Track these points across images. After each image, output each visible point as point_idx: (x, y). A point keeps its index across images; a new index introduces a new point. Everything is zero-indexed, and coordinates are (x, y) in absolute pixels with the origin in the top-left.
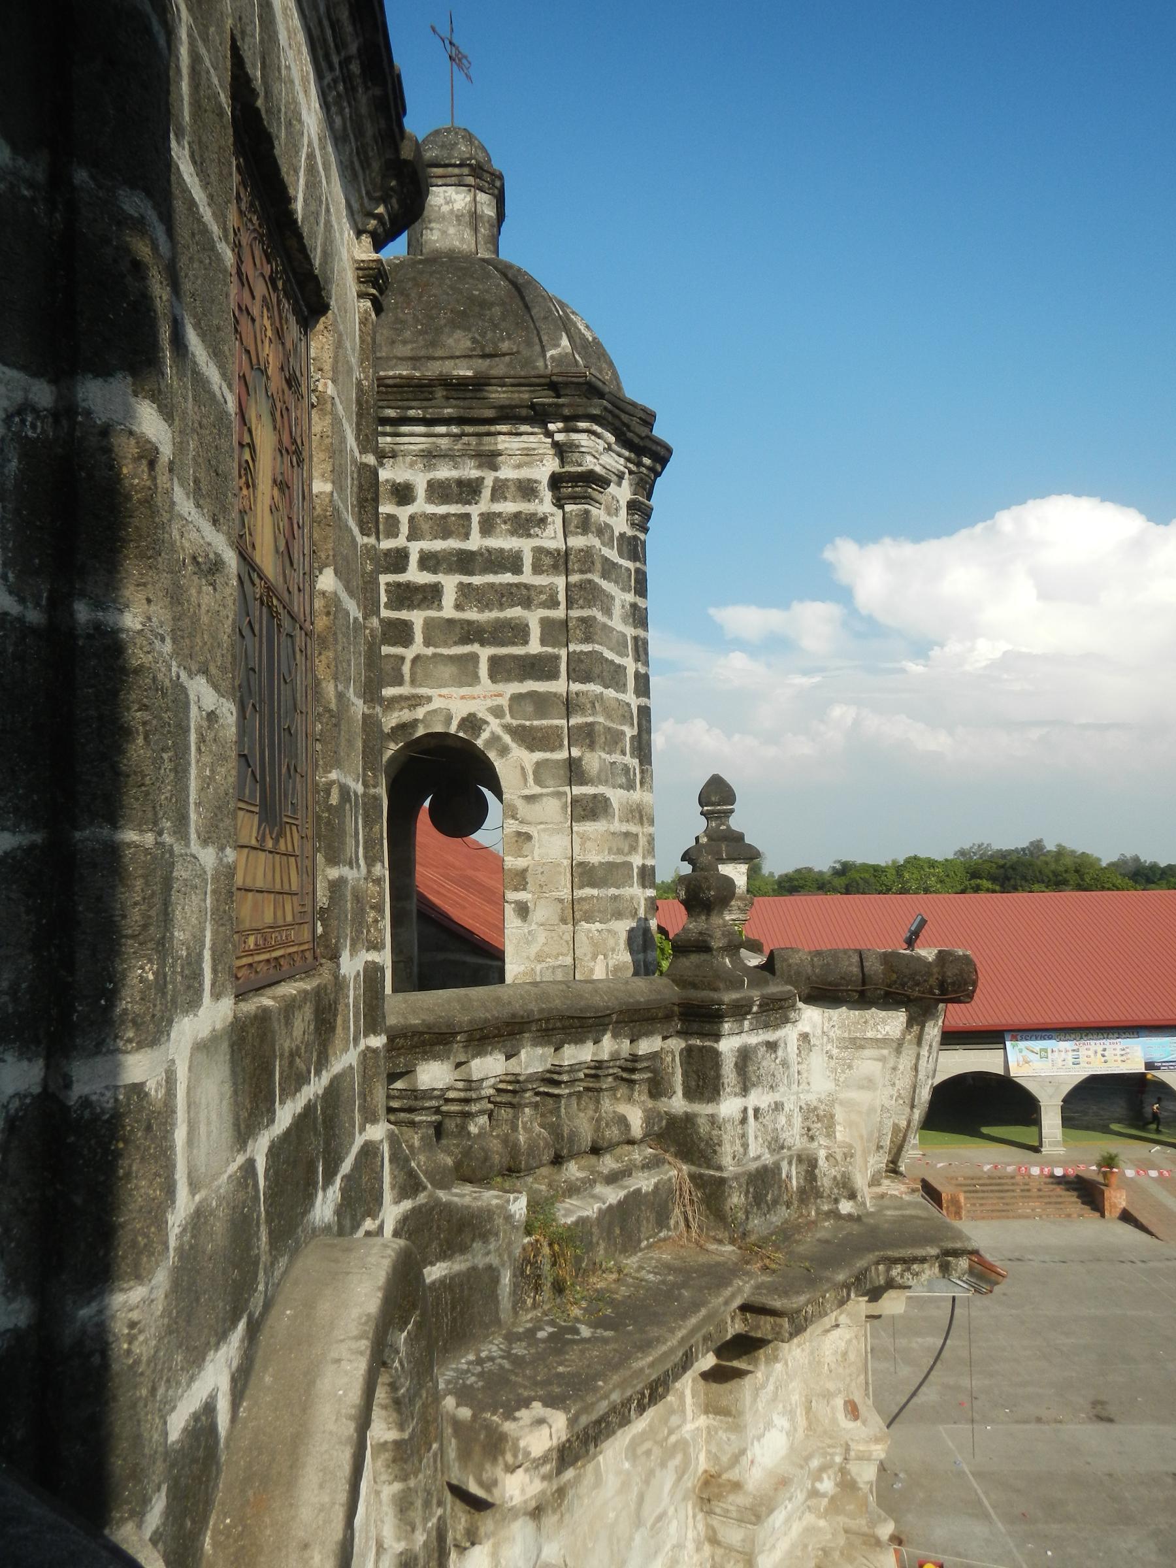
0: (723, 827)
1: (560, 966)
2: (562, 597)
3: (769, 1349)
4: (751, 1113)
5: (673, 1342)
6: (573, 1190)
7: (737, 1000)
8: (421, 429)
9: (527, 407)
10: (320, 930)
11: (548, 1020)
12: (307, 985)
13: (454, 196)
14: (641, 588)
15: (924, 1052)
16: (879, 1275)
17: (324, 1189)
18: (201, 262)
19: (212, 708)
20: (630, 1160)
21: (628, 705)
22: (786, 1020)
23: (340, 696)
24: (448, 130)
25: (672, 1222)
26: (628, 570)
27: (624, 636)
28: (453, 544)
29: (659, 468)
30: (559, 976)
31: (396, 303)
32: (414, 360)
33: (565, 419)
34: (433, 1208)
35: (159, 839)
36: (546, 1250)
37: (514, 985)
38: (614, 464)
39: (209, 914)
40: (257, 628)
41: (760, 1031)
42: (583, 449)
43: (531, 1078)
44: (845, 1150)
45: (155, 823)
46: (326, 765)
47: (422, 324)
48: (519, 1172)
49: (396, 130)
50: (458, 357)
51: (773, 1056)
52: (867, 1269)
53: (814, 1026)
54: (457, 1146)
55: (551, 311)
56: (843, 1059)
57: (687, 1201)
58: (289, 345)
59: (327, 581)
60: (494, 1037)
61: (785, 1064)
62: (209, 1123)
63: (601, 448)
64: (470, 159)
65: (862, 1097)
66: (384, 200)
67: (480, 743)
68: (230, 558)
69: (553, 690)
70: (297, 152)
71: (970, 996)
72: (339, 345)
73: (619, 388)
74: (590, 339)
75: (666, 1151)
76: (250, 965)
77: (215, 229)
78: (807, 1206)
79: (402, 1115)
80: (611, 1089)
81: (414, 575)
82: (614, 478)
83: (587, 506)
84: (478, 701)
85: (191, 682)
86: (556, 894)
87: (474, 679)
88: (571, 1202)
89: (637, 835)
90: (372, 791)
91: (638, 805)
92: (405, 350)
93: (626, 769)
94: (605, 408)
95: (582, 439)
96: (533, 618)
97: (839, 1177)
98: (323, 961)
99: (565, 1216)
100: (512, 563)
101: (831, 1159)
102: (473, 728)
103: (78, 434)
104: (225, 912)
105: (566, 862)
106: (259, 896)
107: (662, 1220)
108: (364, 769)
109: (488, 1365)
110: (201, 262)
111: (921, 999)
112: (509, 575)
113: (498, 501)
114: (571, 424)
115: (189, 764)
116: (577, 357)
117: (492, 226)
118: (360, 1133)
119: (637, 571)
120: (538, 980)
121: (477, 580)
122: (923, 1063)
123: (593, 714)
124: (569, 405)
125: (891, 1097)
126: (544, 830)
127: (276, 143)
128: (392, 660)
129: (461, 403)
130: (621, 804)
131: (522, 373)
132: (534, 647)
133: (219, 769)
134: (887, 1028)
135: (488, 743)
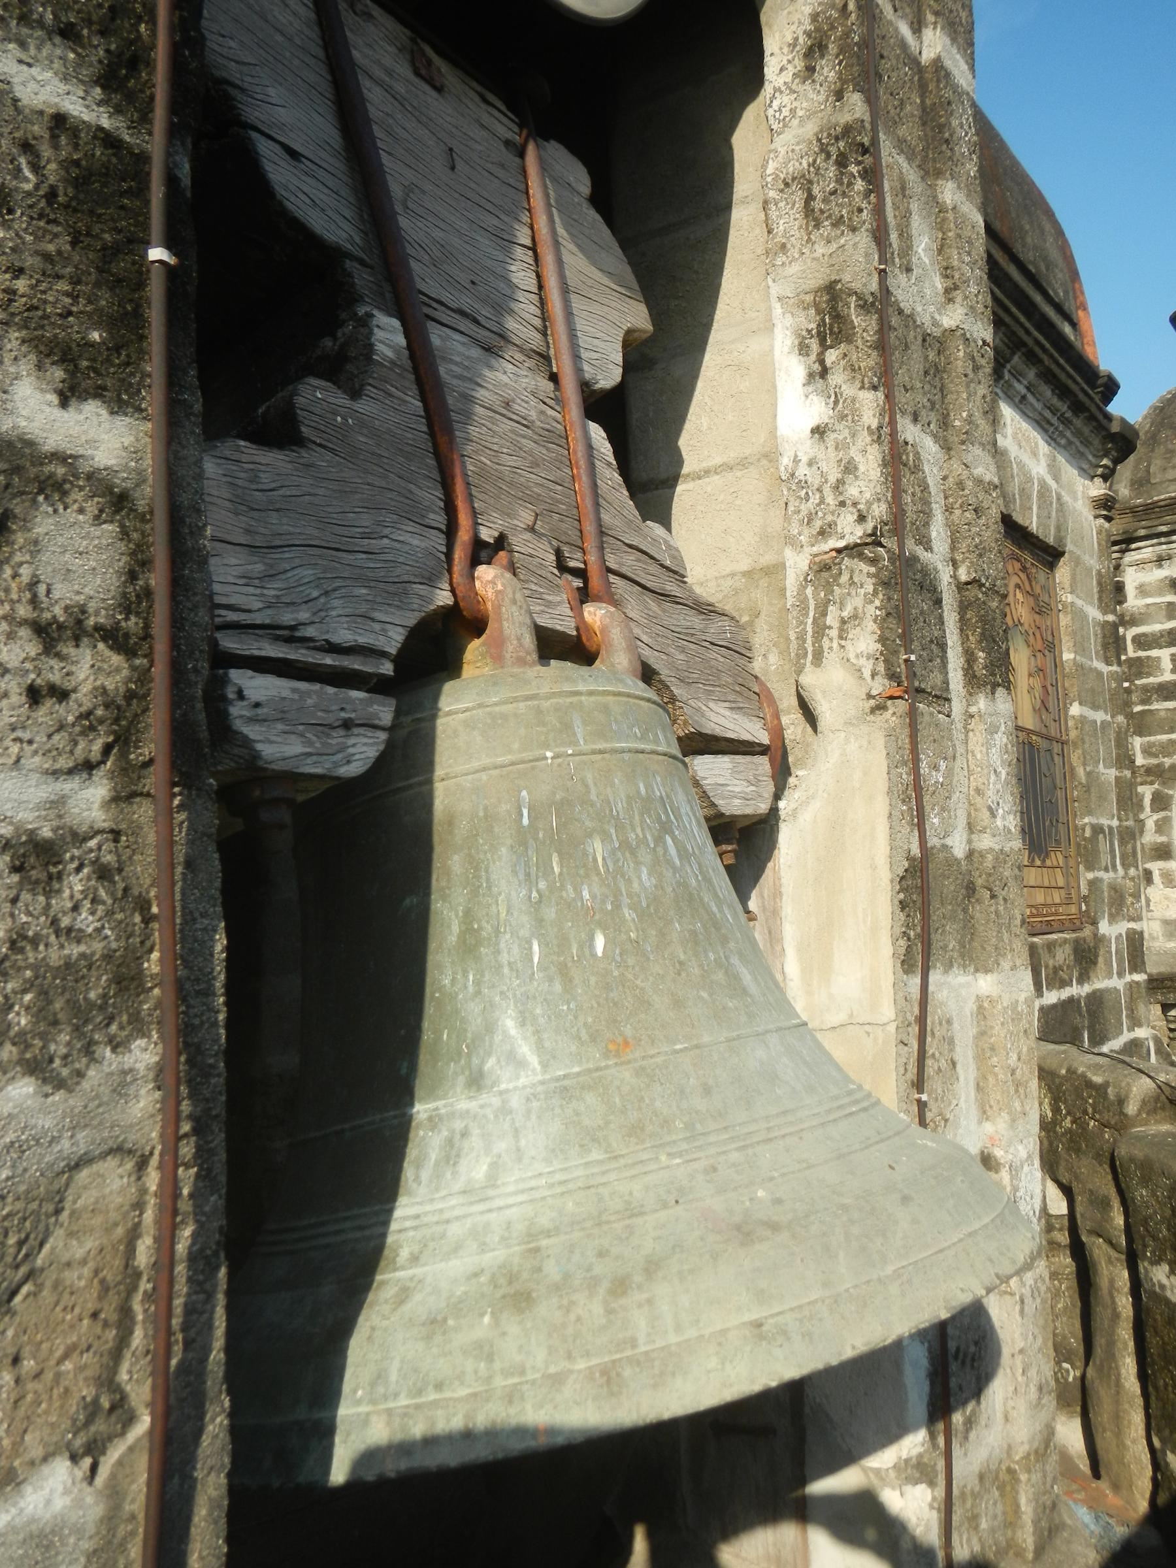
10: (1084, 908)
23: (1088, 774)
58: (1038, 590)
59: (1075, 710)
66: (1105, 455)
72: (1077, 561)
90: (1125, 823)
108: (1119, 810)
118: (1129, 1031)
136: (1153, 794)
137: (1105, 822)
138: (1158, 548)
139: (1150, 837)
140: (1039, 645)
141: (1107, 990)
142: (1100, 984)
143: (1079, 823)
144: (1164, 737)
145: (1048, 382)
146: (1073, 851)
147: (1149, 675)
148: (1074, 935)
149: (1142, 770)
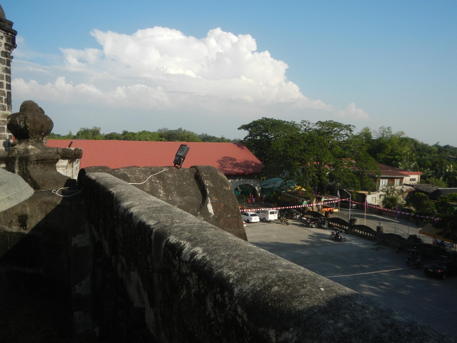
14: (9, 64)
15: (74, 169)
21: (4, 91)
26: (4, 60)
27: (3, 75)
29: (14, 36)
71: (81, 157)
93: (3, 106)
119: (7, 60)
122: (74, 171)
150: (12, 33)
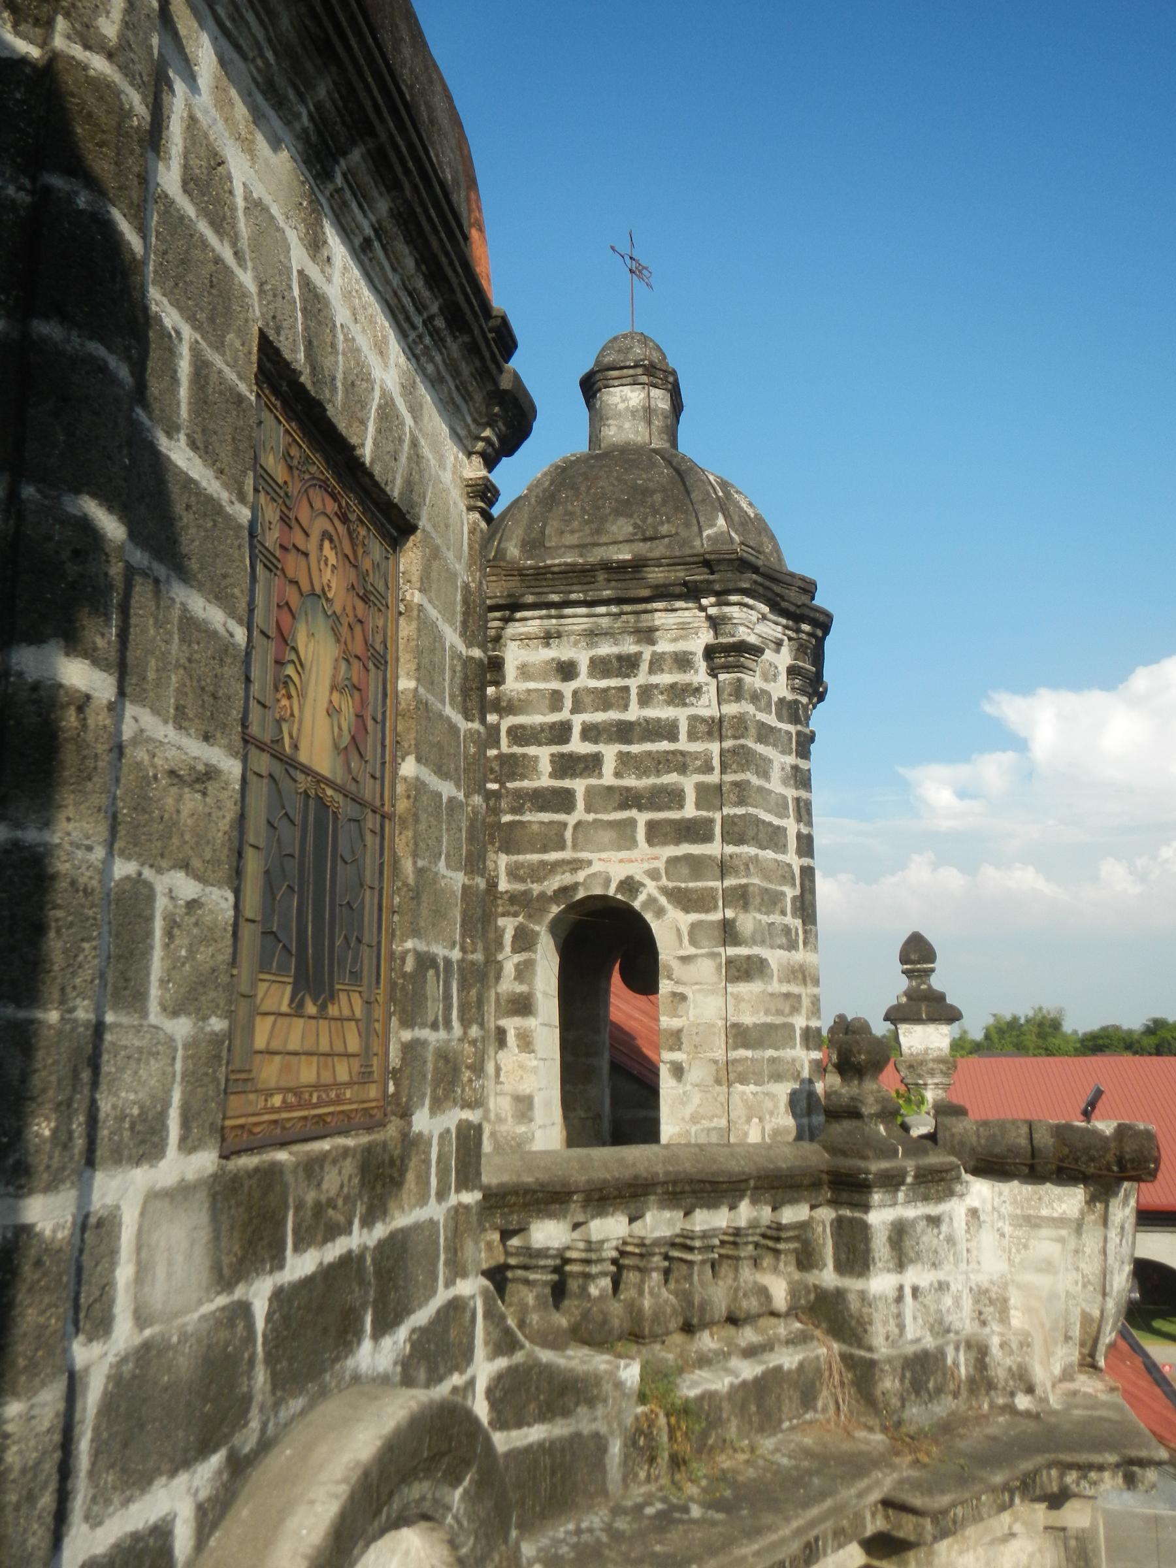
0: (923, 987)
1: (714, 1128)
2: (716, 762)
3: (922, 1553)
4: (908, 1291)
5: (786, 1531)
6: (703, 1361)
7: (887, 1170)
8: (583, 610)
9: (680, 584)
10: (391, 1089)
11: (675, 1183)
12: (350, 1142)
13: (630, 394)
14: (804, 753)
15: (1113, 1234)
16: (1051, 1480)
17: (377, 1336)
18: (199, 527)
19: (195, 896)
20: (775, 1334)
21: (789, 865)
22: (951, 1193)
23: (420, 872)
24: (625, 336)
25: (820, 1404)
26: (788, 733)
27: (785, 798)
28: (613, 715)
29: (819, 633)
30: (714, 1139)
31: (567, 497)
32: (581, 547)
33: (717, 594)
34: (531, 1369)
35: (68, 1016)
36: (662, 1420)
37: (667, 1146)
38: (771, 632)
39: (178, 1078)
40: (298, 819)
41: (919, 1204)
42: (735, 621)
43: (657, 1242)
44: (1021, 1338)
45: (63, 1001)
46: (402, 935)
47: (589, 515)
48: (644, 1338)
49: (492, 367)
50: (621, 542)
51: (936, 1231)
52: (1036, 1472)
53: (984, 1201)
54: (577, 1307)
55: (708, 494)
56: (1019, 1238)
57: (837, 1382)
58: (367, 564)
59: (409, 768)
60: (615, 1198)
61: (950, 1240)
62: (170, 1263)
63: (754, 619)
64: (643, 360)
65: (1043, 1281)
66: (491, 424)
67: (637, 905)
68: (232, 768)
69: (708, 852)
70: (363, 407)
71: (1153, 1175)
72: (434, 554)
73: (780, 559)
74: (752, 515)
75: (817, 1327)
76: (275, 1122)
77: (224, 496)
78: (977, 1398)
79: (520, 1273)
80: (751, 1257)
81: (577, 746)
82: (772, 645)
83: (739, 675)
84: (635, 864)
85: (159, 877)
86: (710, 1055)
87: (632, 843)
88: (699, 1374)
89: (799, 996)
90: (471, 957)
91: (801, 966)
92: (571, 539)
93: (787, 930)
94: (755, 582)
95: (734, 612)
96: (689, 784)
97: (1014, 1368)
98: (393, 1118)
99: (689, 1388)
100: (668, 731)
101: (1007, 1348)
102: (630, 891)
103: (10, 691)
104: (206, 1074)
105: (721, 1023)
106: (294, 1059)
107: (808, 1399)
108: (463, 936)
109: (585, 1537)
110: (199, 527)
111: (1100, 1176)
112: (665, 742)
113: (655, 673)
114: (723, 598)
115: (152, 948)
116: (733, 534)
117: (666, 417)
119: (799, 733)
120: (693, 1141)
121: (635, 749)
122: (1111, 1247)
123: (747, 876)
124: (720, 581)
125: (1076, 1283)
126: (699, 991)
127: (329, 407)
128: (556, 826)
129: (619, 585)
130: (780, 965)
131: (678, 554)
132: (690, 811)
133: (202, 949)
134: (1064, 1206)
135: (645, 905)
136: (516, 929)
137: (440, 950)
138: (546, 622)
139: (508, 985)
140: (358, 647)
141: (417, 1227)
142: (403, 1219)
143: (397, 948)
144: (534, 857)
145: (409, 241)
146: (382, 994)
147: (523, 777)
148: (365, 1139)
149: (506, 897)
150: (814, 623)
